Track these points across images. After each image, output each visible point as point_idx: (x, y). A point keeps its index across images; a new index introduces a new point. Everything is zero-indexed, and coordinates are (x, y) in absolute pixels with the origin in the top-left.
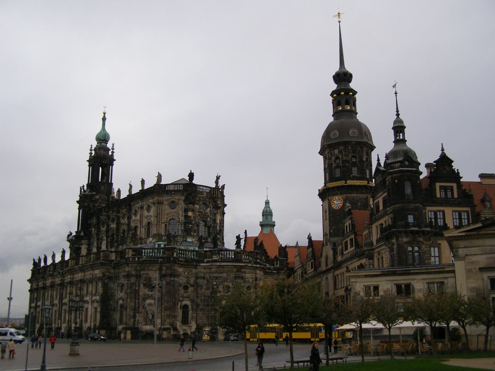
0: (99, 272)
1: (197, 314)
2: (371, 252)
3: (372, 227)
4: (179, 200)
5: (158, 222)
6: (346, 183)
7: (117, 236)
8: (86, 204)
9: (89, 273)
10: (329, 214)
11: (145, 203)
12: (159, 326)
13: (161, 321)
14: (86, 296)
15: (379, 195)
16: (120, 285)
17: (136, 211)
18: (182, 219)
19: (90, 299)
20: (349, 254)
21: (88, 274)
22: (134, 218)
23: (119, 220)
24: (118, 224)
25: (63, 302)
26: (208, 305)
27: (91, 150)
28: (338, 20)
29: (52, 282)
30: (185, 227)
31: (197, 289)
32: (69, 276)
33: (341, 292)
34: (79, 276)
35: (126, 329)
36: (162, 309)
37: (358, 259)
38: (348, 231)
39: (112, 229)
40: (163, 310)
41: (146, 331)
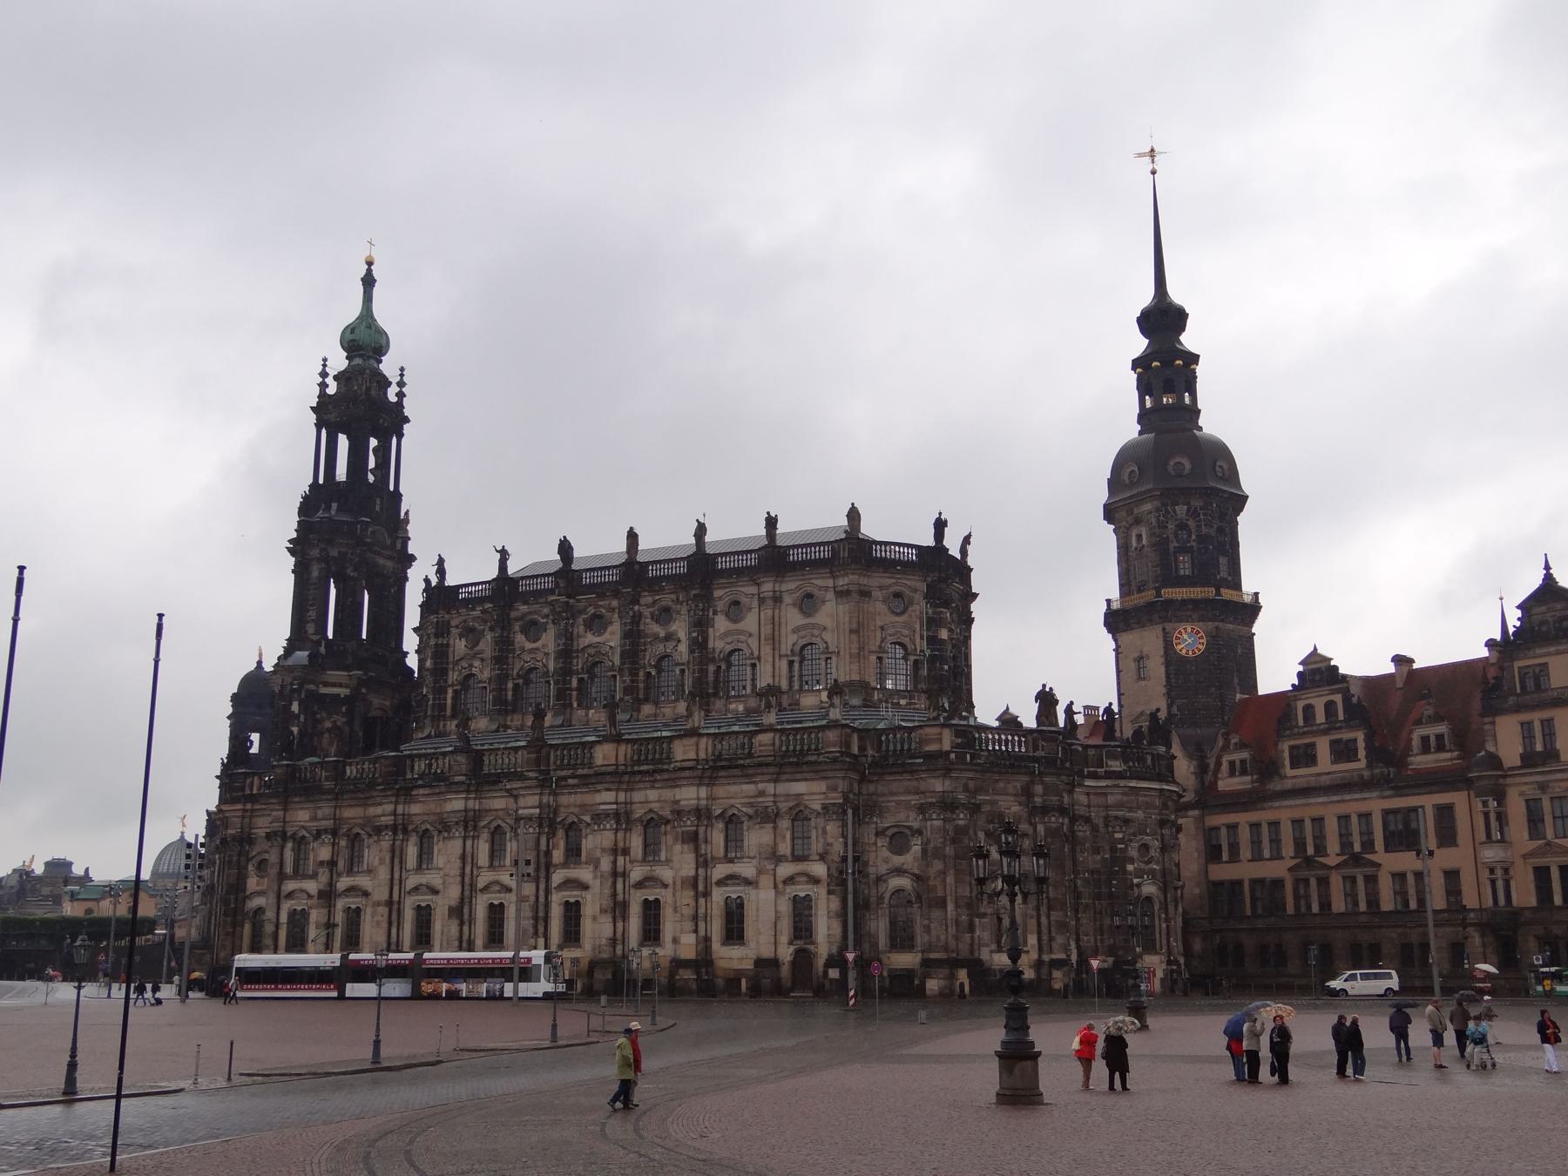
0: (824, 789)
1: (1078, 920)
2: (1501, 781)
3: (1493, 723)
4: (915, 590)
5: (861, 649)
6: (1218, 593)
7: (634, 673)
8: (334, 553)
9: (749, 788)
10: (1168, 664)
11: (790, 586)
12: (1034, 956)
13: (1040, 940)
14: (731, 861)
15: (1552, 649)
16: (890, 833)
17: (736, 603)
18: (921, 644)
19: (760, 872)
20: (1323, 778)
21: (736, 794)
22: (721, 624)
23: (638, 624)
24: (634, 638)
25: (557, 877)
26: (1098, 897)
27: (324, 374)
28: (1150, 167)
29: (466, 810)
30: (929, 670)
31: (1073, 851)
32: (609, 796)
33: (1276, 870)
34: (689, 795)
35: (955, 964)
36: (1038, 909)
37: (1389, 793)
38: (1320, 717)
39: (592, 651)
40: (1044, 909)
41: (1001, 971)
